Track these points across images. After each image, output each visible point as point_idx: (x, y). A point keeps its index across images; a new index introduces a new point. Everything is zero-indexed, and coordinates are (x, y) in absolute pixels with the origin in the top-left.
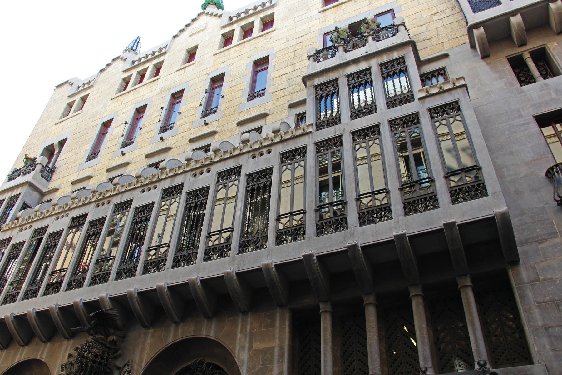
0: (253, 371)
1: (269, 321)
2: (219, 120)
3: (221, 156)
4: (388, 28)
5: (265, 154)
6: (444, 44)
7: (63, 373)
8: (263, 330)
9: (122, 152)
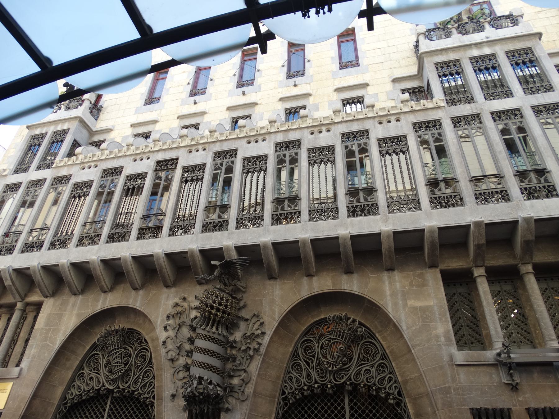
0: (414, 328)
1: (420, 280)
2: (310, 83)
3: (343, 118)
4: (506, 17)
5: (393, 122)
6: (556, 42)
7: (169, 322)
8: (415, 288)
9: (195, 100)
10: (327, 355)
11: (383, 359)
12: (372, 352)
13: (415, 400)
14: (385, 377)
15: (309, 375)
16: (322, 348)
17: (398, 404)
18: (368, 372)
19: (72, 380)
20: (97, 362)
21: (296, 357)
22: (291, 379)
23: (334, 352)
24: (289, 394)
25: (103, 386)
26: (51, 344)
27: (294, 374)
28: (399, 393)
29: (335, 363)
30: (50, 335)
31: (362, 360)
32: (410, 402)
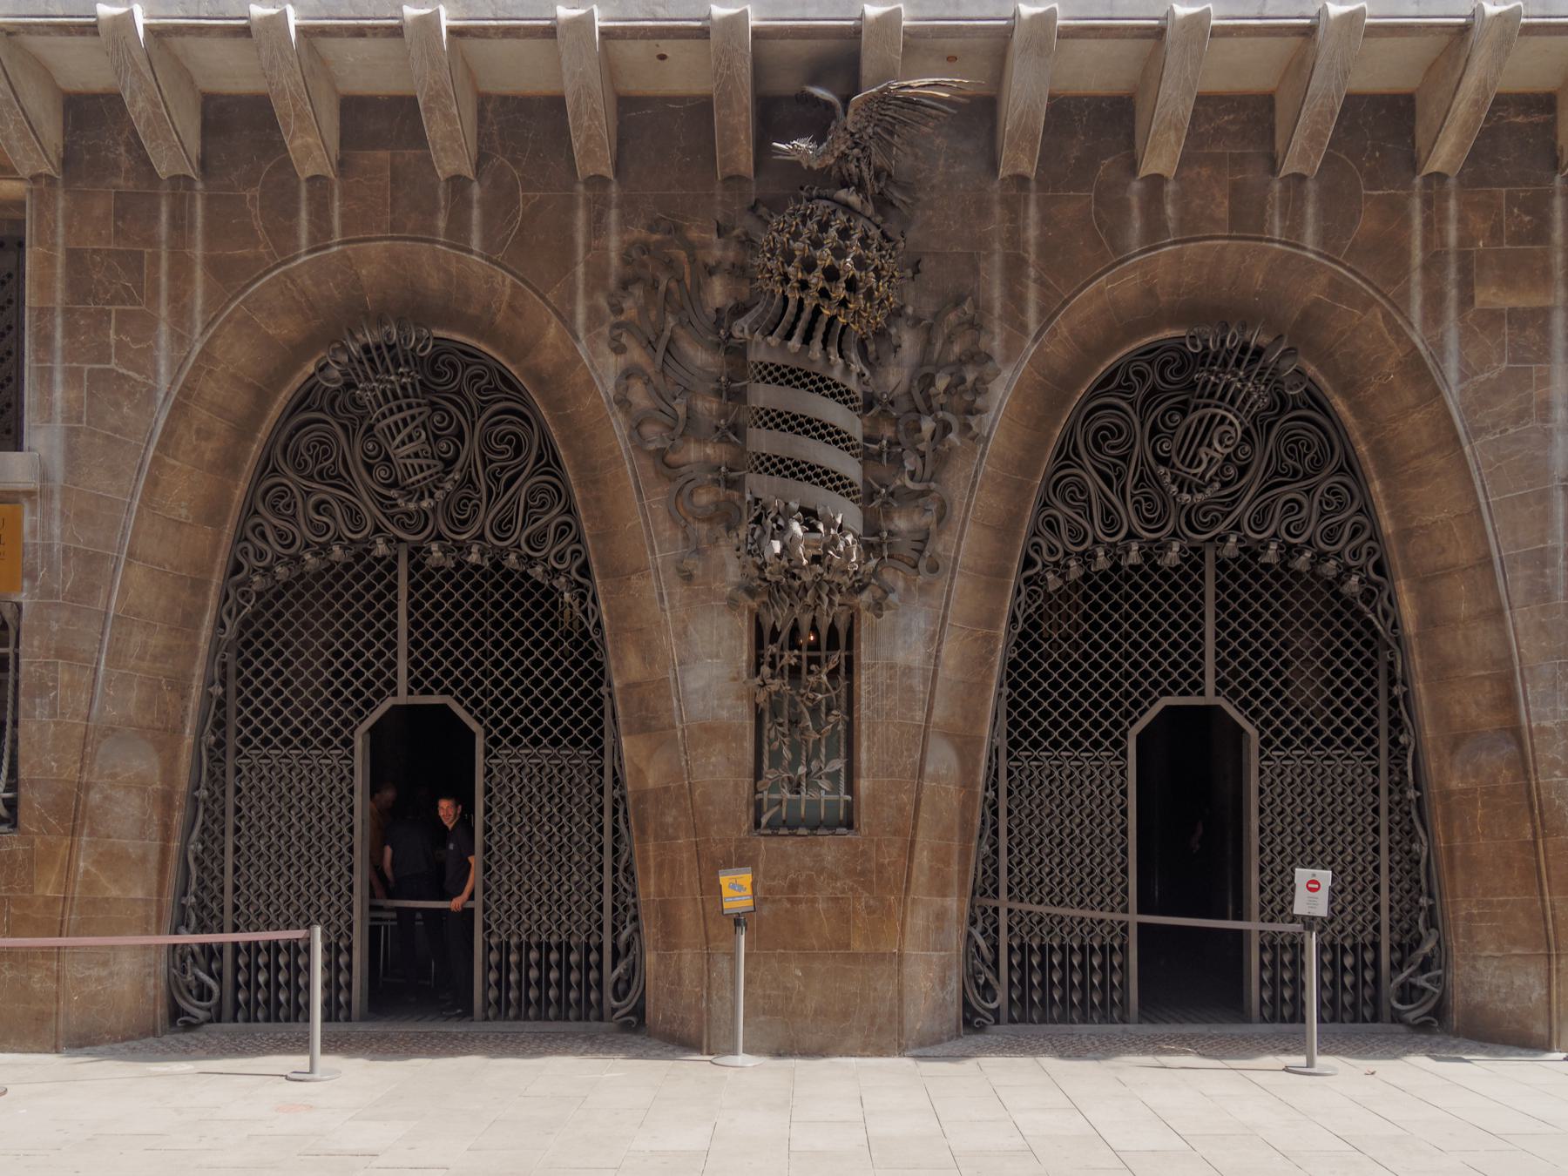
10: (1174, 453)
11: (1341, 469)
12: (1309, 448)
13: (1424, 583)
14: (1341, 525)
15: (1109, 513)
16: (1154, 431)
17: (1368, 597)
18: (1293, 508)
21: (1067, 457)
22: (1052, 525)
23: (1200, 444)
24: (1044, 566)
26: (131, 373)
27: (1061, 511)
28: (1379, 568)
29: (1196, 480)
31: (1276, 473)
32: (1410, 589)
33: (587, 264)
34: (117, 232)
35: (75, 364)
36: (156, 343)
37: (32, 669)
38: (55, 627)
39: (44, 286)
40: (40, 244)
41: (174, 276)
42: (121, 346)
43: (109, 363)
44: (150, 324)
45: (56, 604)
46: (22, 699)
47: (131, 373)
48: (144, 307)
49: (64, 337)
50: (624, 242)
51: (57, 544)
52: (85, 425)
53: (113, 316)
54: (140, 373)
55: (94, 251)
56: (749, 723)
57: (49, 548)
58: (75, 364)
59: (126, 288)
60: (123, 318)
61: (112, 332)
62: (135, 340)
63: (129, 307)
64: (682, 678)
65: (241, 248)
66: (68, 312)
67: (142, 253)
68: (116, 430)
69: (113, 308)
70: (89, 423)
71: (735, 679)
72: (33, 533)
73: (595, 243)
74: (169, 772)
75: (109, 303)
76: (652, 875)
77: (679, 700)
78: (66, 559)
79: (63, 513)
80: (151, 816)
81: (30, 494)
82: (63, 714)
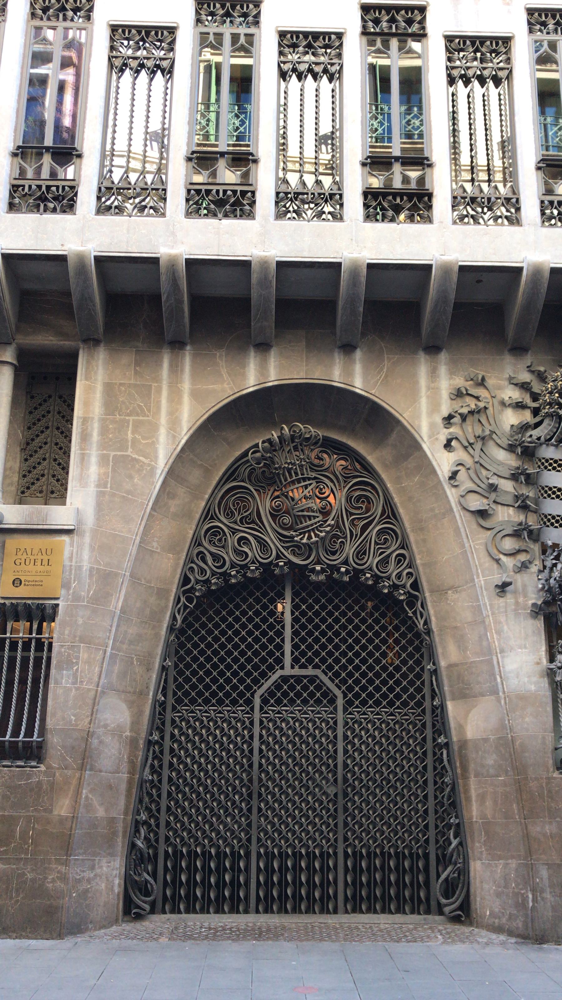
19: (196, 542)
20: (245, 507)
25: (278, 557)
26: (141, 458)
30: (130, 435)
33: (428, 397)
34: (136, 373)
35: (105, 452)
36: (157, 440)
37: (63, 650)
38: (80, 621)
39: (87, 404)
40: (86, 379)
41: (171, 400)
42: (134, 441)
43: (126, 451)
44: (154, 428)
45: (82, 606)
46: (53, 671)
47: (141, 458)
48: (150, 418)
49: (98, 435)
50: (450, 385)
51: (86, 565)
52: (109, 489)
53: (131, 423)
54: (146, 458)
55: (121, 384)
56: (549, 694)
57: (79, 568)
58: (105, 452)
59: (139, 406)
60: (137, 425)
61: (129, 432)
62: (144, 438)
63: (141, 418)
64: (503, 662)
65: (213, 384)
66: (102, 421)
67: (151, 386)
68: (128, 492)
69: (131, 418)
70: (111, 488)
71: (538, 664)
72: (71, 559)
73: (433, 385)
74: (135, 724)
75: (128, 415)
76: (474, 803)
77: (501, 677)
78: (91, 576)
79: (91, 546)
80: (123, 756)
81: (68, 532)
82: (82, 682)
